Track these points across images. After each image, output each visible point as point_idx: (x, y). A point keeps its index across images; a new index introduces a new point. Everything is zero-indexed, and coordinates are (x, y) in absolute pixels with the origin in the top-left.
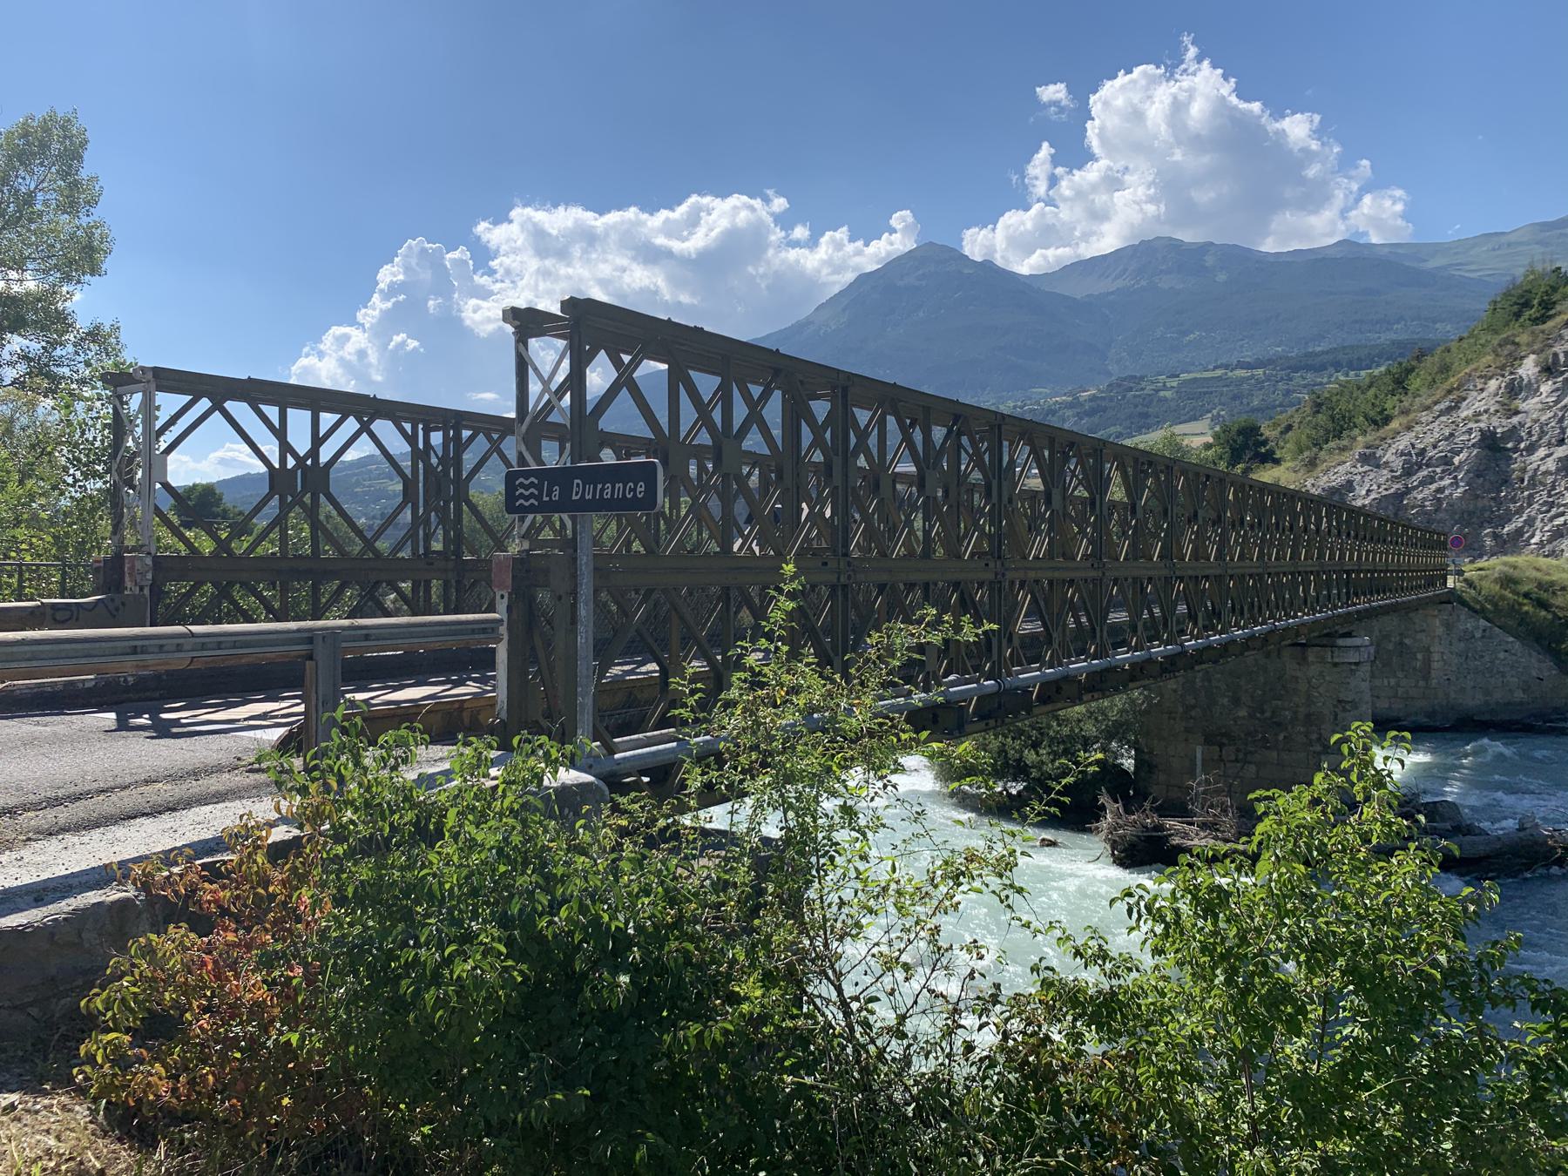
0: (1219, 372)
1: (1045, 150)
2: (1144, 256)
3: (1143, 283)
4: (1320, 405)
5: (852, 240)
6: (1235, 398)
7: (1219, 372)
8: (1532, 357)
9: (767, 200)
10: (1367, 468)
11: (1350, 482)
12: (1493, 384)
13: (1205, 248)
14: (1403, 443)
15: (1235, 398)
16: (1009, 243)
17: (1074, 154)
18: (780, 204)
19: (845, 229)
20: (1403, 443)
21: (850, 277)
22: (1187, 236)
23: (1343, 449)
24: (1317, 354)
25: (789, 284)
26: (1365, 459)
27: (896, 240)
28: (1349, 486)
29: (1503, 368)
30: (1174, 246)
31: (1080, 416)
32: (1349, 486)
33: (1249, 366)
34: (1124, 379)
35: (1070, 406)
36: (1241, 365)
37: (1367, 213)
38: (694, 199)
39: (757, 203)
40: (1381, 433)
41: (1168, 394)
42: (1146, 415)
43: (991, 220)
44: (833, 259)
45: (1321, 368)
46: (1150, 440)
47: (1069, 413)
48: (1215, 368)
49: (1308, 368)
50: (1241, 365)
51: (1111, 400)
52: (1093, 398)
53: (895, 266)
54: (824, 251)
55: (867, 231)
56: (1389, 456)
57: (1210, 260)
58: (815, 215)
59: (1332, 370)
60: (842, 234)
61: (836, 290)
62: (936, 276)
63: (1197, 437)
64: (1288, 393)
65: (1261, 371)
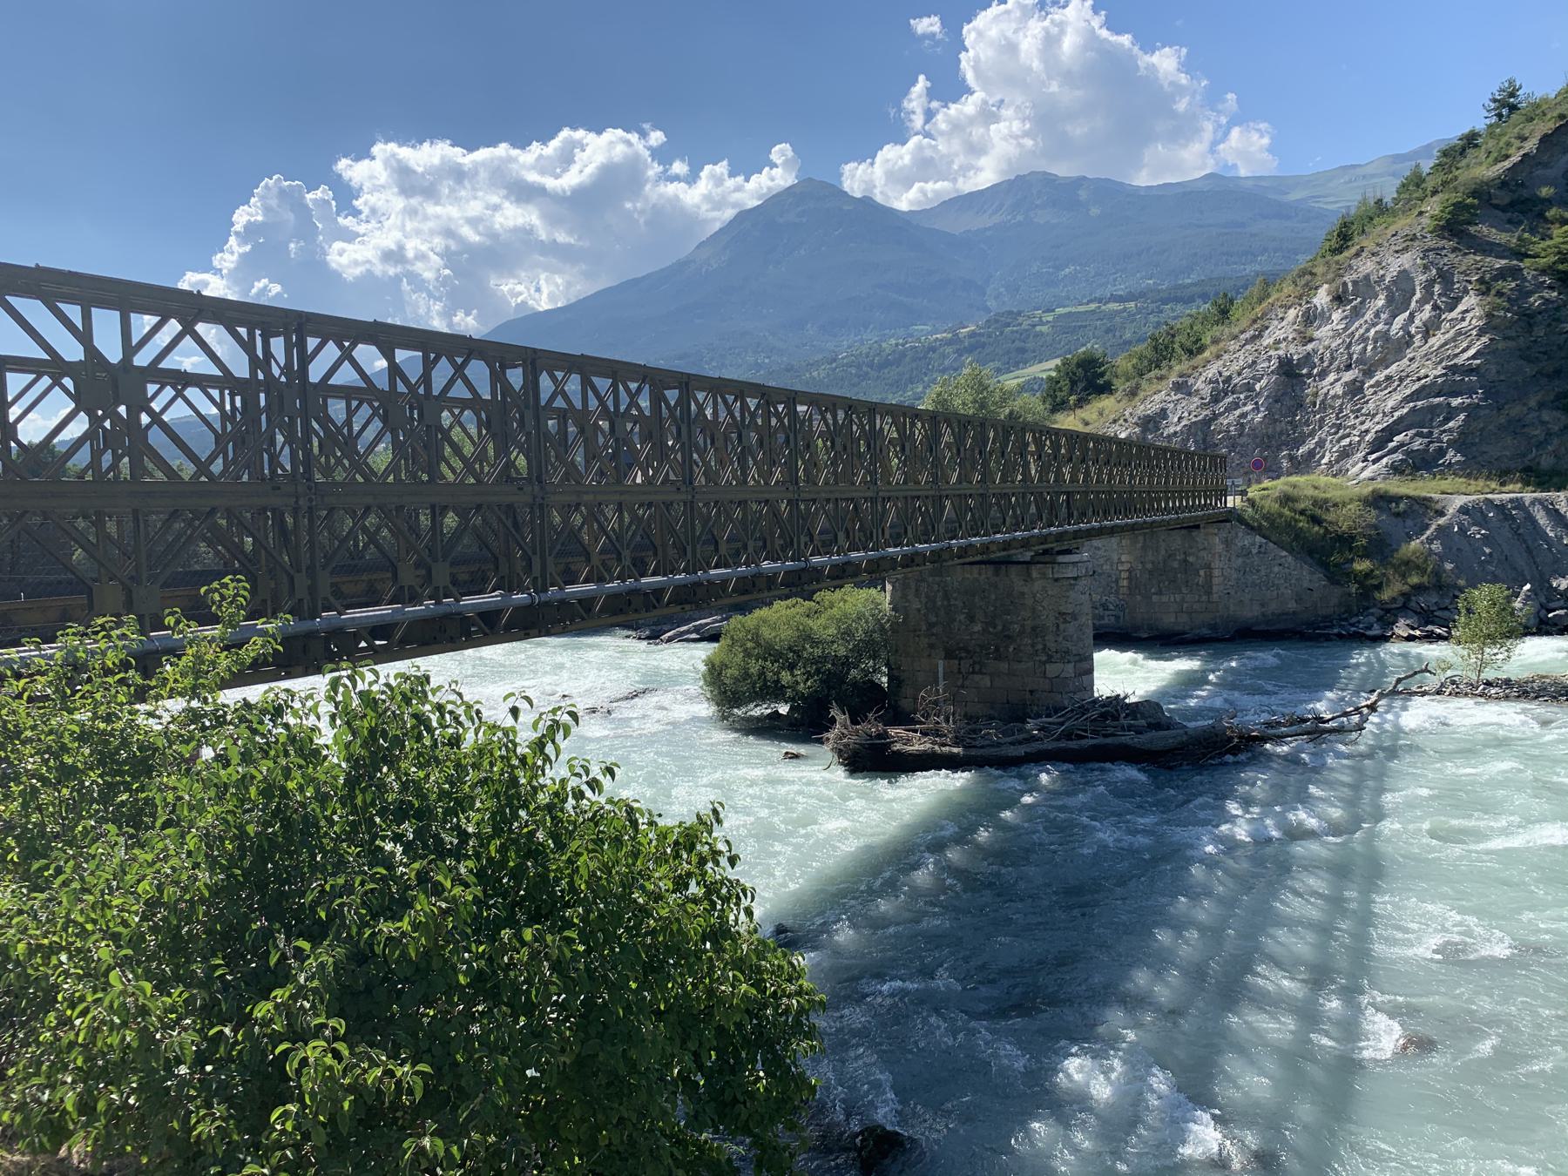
0: (1093, 306)
1: (922, 83)
2: (1020, 190)
3: (1020, 218)
5: (732, 175)
6: (1108, 331)
7: (1093, 306)
8: (1326, 286)
9: (643, 135)
10: (1179, 396)
11: (1164, 410)
12: (1292, 313)
14: (1211, 372)
15: (1108, 331)
16: (884, 177)
17: (949, 88)
18: (657, 137)
19: (725, 163)
20: (1211, 372)
21: (729, 214)
23: (1161, 378)
25: (668, 218)
26: (1178, 387)
27: (777, 175)
28: (1163, 413)
29: (1300, 298)
30: (1048, 180)
32: (1163, 413)
33: (1120, 299)
35: (949, 342)
38: (565, 133)
39: (633, 137)
40: (1194, 362)
41: (1044, 329)
43: (867, 154)
44: (712, 194)
47: (949, 350)
49: (1177, 300)
52: (972, 335)
53: (776, 202)
54: (704, 185)
55: (746, 166)
56: (1199, 384)
57: (1083, 194)
58: (691, 146)
59: (1199, 302)
60: (722, 168)
61: (717, 226)
62: (816, 210)
65: (1132, 304)
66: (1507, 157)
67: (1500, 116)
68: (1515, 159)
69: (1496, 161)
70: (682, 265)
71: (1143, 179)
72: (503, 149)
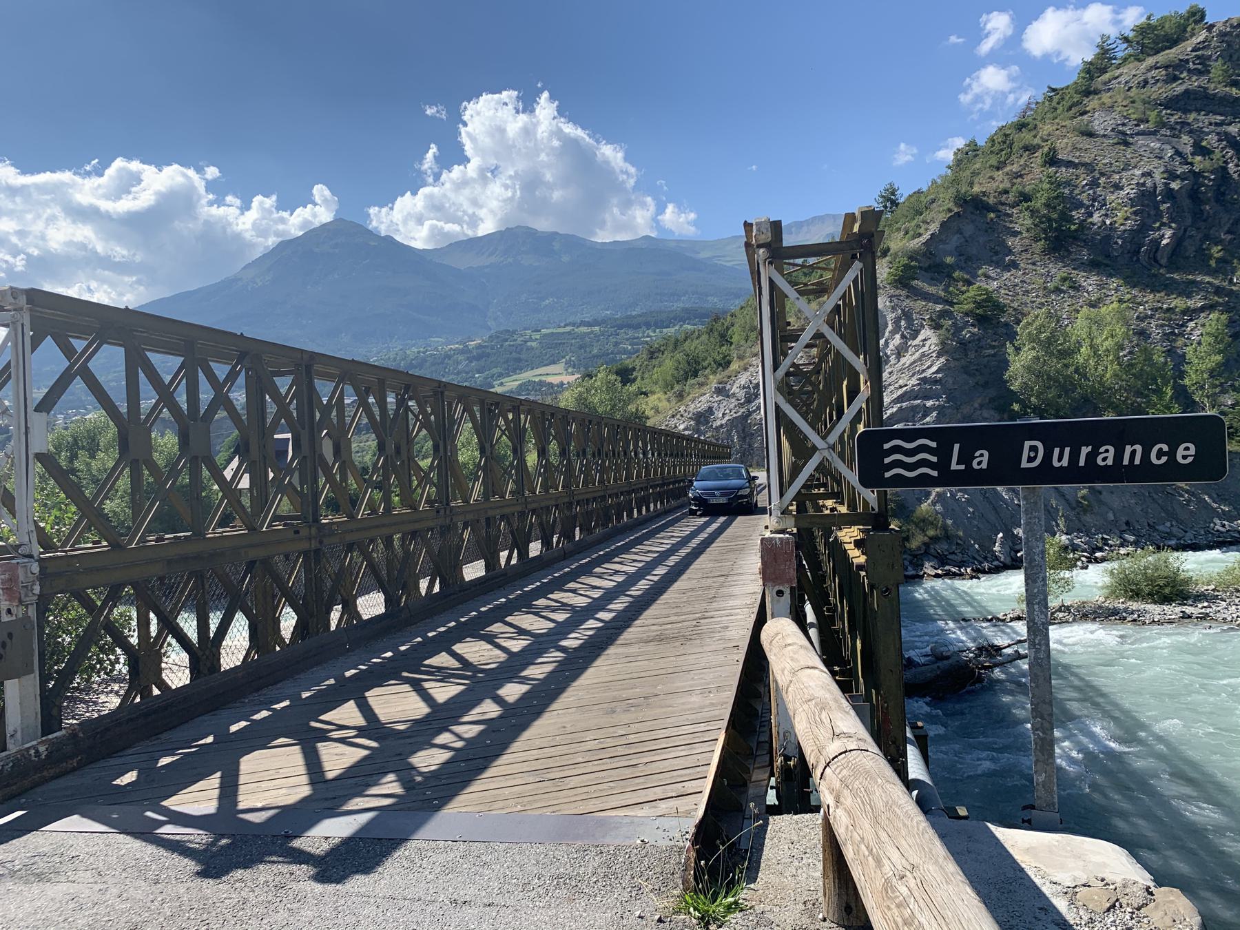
0: (568, 329)
1: (433, 150)
2: (511, 239)
3: (510, 260)
4: (653, 353)
5: (278, 208)
6: (581, 347)
7: (568, 329)
9: (200, 170)
10: (720, 398)
11: (710, 408)
13: (554, 235)
14: (743, 379)
15: (581, 347)
16: (409, 220)
17: (453, 155)
18: (212, 172)
19: (274, 198)
20: (743, 379)
21: (272, 241)
22: (543, 225)
23: (701, 385)
24: (634, 317)
25: (217, 240)
26: (719, 391)
27: (319, 210)
28: (710, 410)
30: (531, 233)
31: (470, 360)
32: (710, 410)
33: (589, 324)
34: (501, 332)
35: (462, 352)
36: (583, 323)
37: (636, 220)
38: (119, 163)
39: (191, 173)
40: (727, 372)
41: (534, 344)
42: (519, 360)
43: (388, 200)
44: (256, 222)
45: (637, 327)
46: (507, 385)
47: (461, 357)
48: (566, 325)
49: (629, 326)
50: (583, 323)
51: (492, 348)
52: (479, 347)
53: (315, 235)
54: (253, 215)
55: (288, 204)
56: (735, 389)
57: (556, 246)
58: (239, 185)
59: (644, 328)
60: (270, 202)
61: (258, 254)
62: (349, 244)
63: (560, 380)
64: (616, 344)
65: (597, 328)
66: (920, 235)
67: (885, 207)
68: (926, 236)
69: (914, 238)
70: (234, 280)
71: (603, 237)
72: (65, 176)
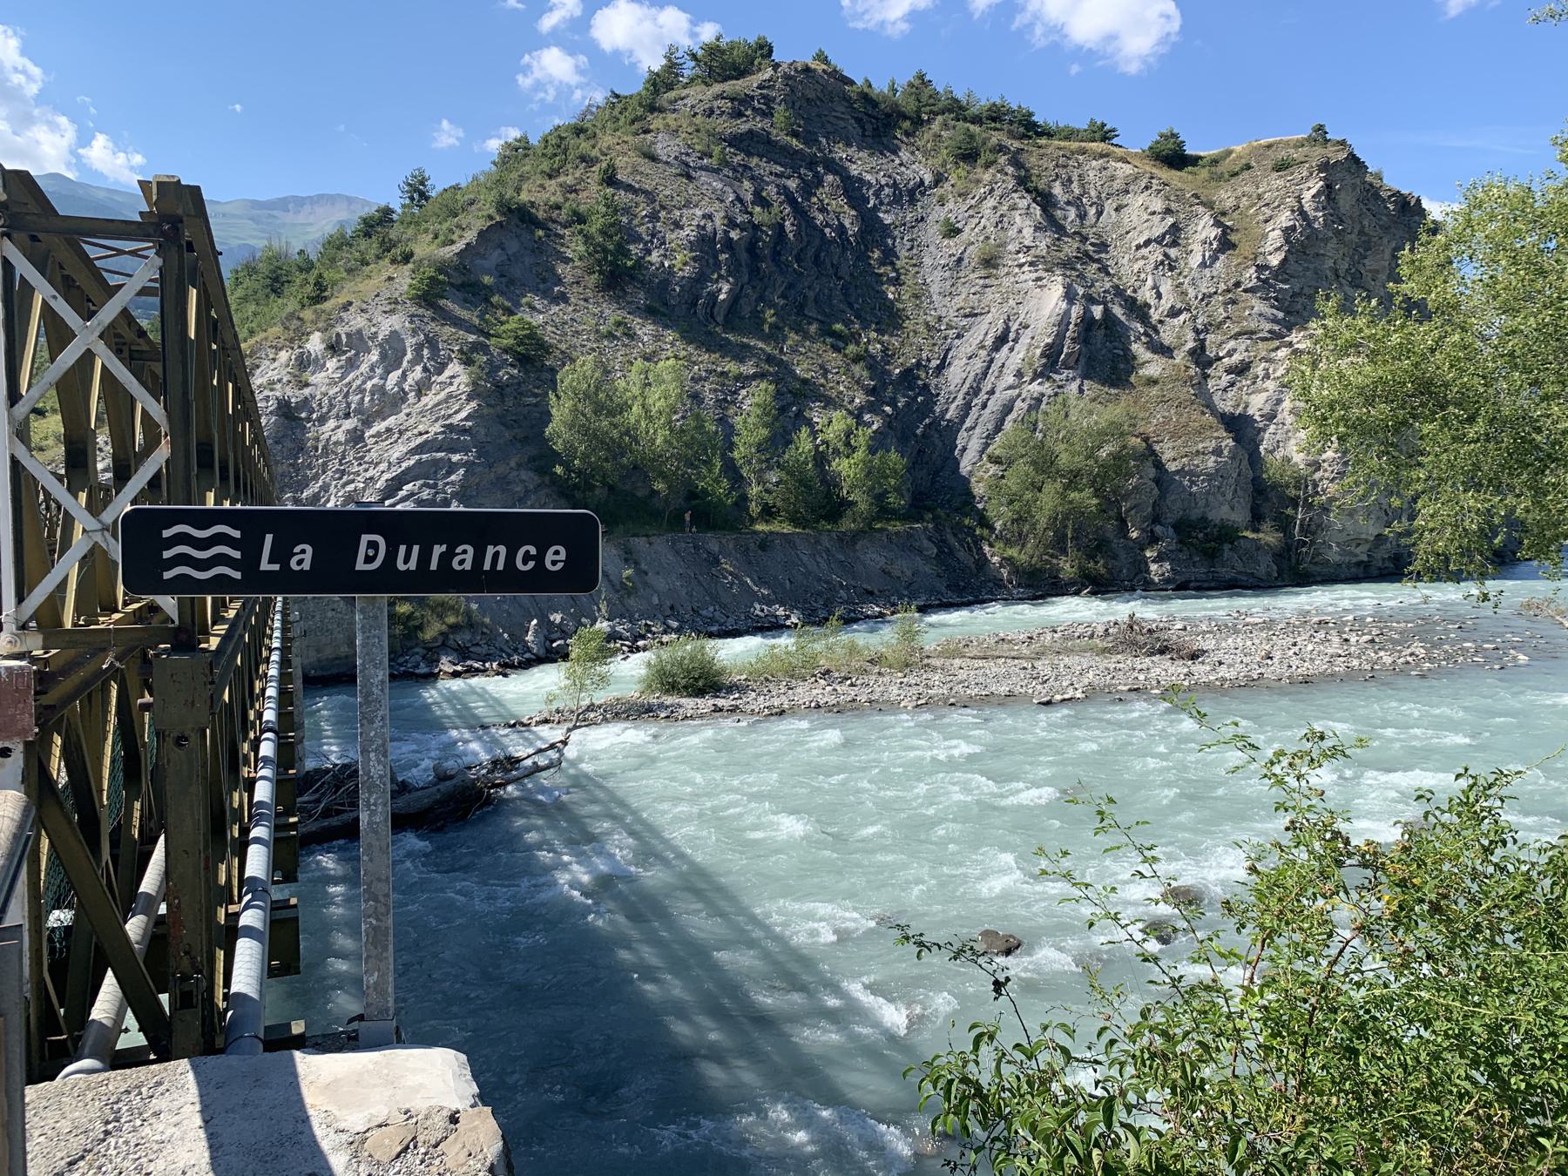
8: (318, 334)
12: (284, 356)
29: (292, 340)
66: (453, 242)
67: (412, 199)
68: (460, 246)
69: (444, 244)
